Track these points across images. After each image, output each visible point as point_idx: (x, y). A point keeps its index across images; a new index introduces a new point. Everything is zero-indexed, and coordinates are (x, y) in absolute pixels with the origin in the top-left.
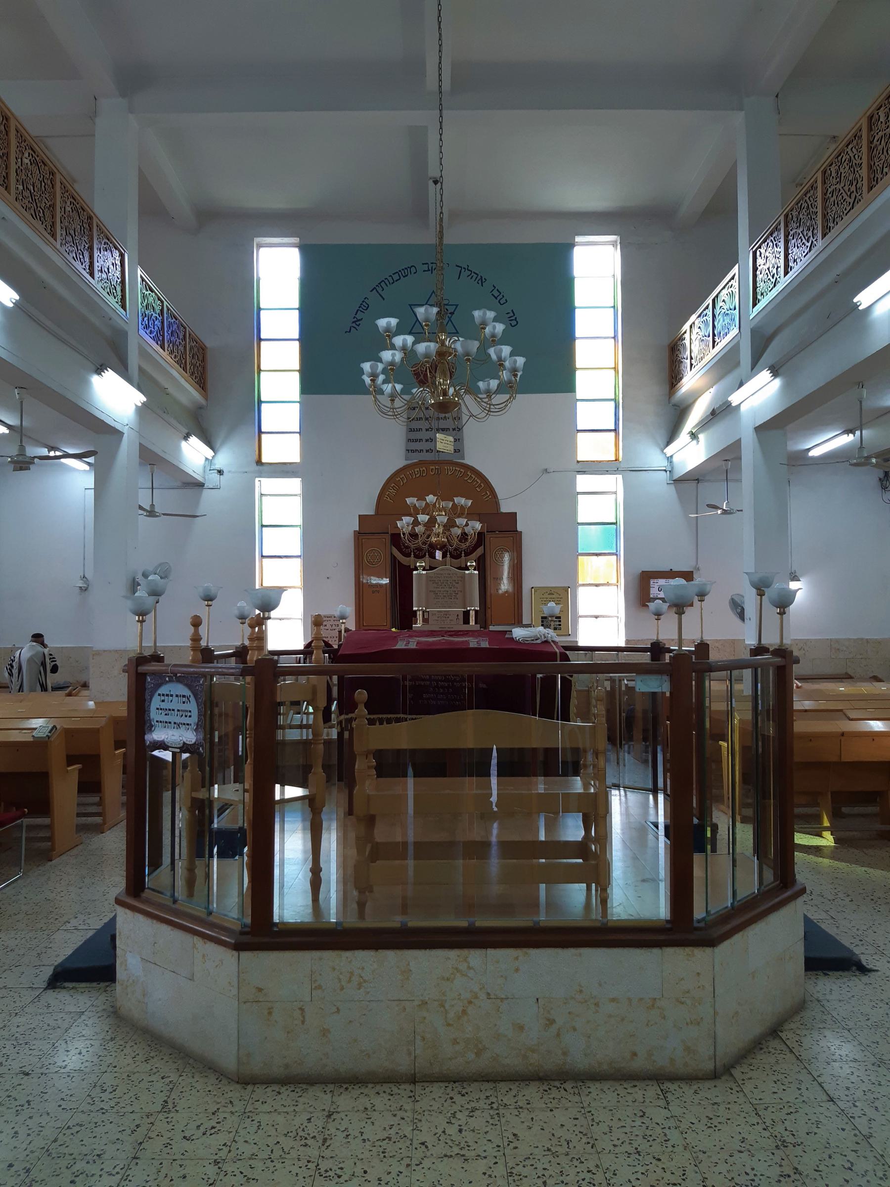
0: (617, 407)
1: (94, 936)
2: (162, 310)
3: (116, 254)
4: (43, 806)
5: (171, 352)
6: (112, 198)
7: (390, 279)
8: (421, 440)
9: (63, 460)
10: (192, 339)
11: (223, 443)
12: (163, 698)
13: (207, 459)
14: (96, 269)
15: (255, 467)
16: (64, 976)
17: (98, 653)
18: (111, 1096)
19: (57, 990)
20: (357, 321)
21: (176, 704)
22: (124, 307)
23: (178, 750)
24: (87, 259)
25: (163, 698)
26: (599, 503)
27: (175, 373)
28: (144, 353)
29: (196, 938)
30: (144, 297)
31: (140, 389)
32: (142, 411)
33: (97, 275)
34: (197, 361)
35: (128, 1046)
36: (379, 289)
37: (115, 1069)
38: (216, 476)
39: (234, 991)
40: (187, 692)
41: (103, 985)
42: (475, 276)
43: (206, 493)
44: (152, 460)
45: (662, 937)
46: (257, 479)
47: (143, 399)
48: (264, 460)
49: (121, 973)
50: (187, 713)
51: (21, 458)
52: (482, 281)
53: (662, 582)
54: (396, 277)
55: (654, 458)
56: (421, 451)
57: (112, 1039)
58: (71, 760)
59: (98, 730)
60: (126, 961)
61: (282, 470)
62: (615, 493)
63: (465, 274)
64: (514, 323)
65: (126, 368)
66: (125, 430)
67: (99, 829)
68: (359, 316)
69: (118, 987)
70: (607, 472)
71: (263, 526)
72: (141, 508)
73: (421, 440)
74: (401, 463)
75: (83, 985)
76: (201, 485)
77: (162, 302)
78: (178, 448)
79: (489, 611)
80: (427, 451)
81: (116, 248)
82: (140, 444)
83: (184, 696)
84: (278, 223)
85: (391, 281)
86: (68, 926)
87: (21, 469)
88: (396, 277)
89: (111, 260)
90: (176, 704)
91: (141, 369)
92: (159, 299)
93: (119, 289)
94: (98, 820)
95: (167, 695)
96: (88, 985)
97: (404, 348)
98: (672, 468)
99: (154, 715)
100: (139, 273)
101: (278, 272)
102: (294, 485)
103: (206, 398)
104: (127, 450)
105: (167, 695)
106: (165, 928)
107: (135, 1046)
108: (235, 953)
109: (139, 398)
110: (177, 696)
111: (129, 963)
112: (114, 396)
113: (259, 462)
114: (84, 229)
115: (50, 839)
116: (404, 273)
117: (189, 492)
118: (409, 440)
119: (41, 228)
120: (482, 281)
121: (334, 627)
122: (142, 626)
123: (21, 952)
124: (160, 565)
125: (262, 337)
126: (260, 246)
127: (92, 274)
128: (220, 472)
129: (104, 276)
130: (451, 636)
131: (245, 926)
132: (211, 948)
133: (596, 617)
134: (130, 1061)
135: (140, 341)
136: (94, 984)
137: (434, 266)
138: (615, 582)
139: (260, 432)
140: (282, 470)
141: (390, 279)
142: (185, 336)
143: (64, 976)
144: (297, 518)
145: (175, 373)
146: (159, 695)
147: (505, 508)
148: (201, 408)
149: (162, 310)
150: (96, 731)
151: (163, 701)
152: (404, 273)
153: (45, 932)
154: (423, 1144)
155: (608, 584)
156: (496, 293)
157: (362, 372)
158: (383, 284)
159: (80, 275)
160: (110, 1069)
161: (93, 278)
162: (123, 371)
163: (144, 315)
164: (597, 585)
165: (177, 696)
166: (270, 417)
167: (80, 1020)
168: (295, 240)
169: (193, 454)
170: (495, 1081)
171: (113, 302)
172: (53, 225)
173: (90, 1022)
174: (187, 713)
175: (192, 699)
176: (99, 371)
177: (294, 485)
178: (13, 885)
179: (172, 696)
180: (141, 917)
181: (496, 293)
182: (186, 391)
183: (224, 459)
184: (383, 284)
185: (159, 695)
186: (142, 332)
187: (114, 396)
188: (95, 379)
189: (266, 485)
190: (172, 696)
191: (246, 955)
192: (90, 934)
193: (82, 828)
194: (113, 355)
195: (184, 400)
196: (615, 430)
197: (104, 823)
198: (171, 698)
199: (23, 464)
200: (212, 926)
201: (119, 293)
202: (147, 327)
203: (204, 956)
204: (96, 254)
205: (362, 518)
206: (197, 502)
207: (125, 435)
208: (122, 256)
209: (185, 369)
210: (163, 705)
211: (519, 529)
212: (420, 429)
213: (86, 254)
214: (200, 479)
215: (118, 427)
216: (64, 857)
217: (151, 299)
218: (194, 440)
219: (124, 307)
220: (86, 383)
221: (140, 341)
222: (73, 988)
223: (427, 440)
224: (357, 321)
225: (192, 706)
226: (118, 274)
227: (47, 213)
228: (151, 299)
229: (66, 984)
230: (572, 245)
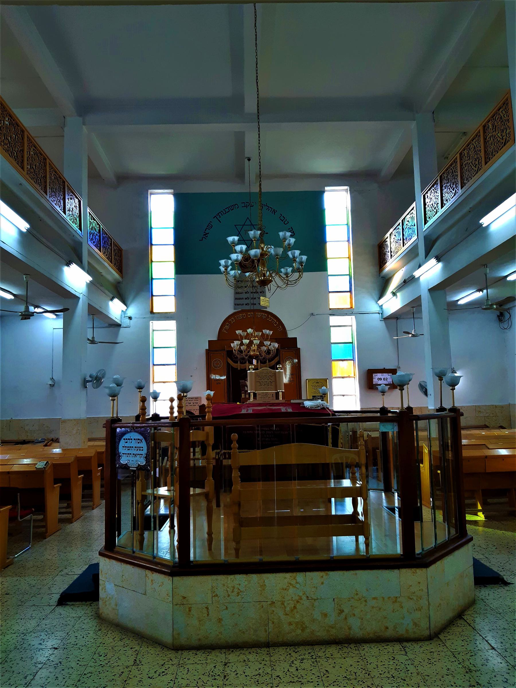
0: (350, 279)
1: (77, 579)
2: (100, 230)
3: (77, 200)
4: (41, 508)
5: (104, 253)
6: (75, 172)
7: (224, 211)
8: (242, 299)
9: (44, 314)
10: (115, 245)
11: (131, 302)
12: (126, 441)
13: (122, 311)
14: (67, 209)
15: (149, 315)
16: (66, 599)
17: (64, 421)
18: (105, 658)
19: (64, 606)
21: (134, 444)
22: (80, 229)
23: (135, 469)
24: (62, 205)
25: (126, 441)
26: (342, 331)
27: (106, 264)
28: (91, 254)
29: (147, 571)
30: (90, 223)
31: (89, 273)
32: (90, 286)
33: (67, 212)
34: (118, 257)
35: (109, 633)
36: (218, 217)
37: (104, 645)
38: (128, 320)
39: (170, 599)
40: (140, 437)
41: (88, 603)
42: (271, 209)
43: (122, 330)
44: (95, 313)
45: (399, 563)
46: (151, 322)
47: (91, 279)
48: (155, 311)
49: (102, 594)
50: (140, 448)
51: (26, 313)
52: (274, 212)
53: (379, 375)
55: (372, 306)
56: (243, 304)
57: (100, 630)
58: (56, 481)
59: (69, 464)
60: (105, 587)
61: (165, 316)
62: (351, 326)
63: (265, 208)
65: (81, 262)
66: (81, 296)
67: (70, 521)
68: (207, 232)
69: (101, 602)
70: (346, 314)
71: (154, 348)
72: (88, 339)
73: (242, 299)
74: (230, 311)
75: (78, 603)
76: (119, 326)
77: (100, 226)
78: (107, 305)
80: (246, 304)
81: (77, 198)
82: (89, 305)
83: (139, 439)
84: (162, 182)
86: (63, 573)
87: (25, 319)
89: (74, 204)
90: (134, 444)
91: (89, 263)
92: (98, 224)
93: (78, 219)
94: (69, 516)
95: (129, 439)
96: (80, 603)
97: (241, 252)
98: (383, 312)
99: (121, 450)
100: (88, 210)
101: (162, 208)
102: (172, 324)
103: (122, 277)
104: (81, 308)
105: (129, 439)
106: (129, 567)
107: (113, 633)
108: (171, 578)
109: (89, 278)
110: (135, 439)
111: (107, 588)
112: (75, 278)
113: (152, 312)
114: (62, 188)
115: (45, 526)
116: (232, 208)
117: (116, 329)
118: (236, 299)
119: (39, 188)
120: (274, 212)
121: (195, 404)
122: (113, 402)
123: (39, 587)
124: (99, 371)
125: (153, 243)
126: (151, 194)
127: (65, 213)
128: (130, 318)
129: (71, 213)
130: (270, 406)
131: (175, 563)
132: (156, 576)
133: (343, 396)
134: (112, 640)
135: (89, 247)
136: (84, 603)
138: (353, 375)
139: (152, 296)
140: (165, 316)
141: (224, 211)
142: (111, 244)
143: (66, 599)
144: (173, 342)
145: (106, 264)
146: (124, 439)
147: (290, 335)
148: (119, 283)
149: (100, 230)
150: (69, 465)
151: (127, 442)
152: (232, 208)
153: (51, 576)
154: (278, 676)
155: (349, 377)
156: (283, 219)
157: (220, 265)
158: (220, 214)
159: (58, 213)
160: (101, 645)
161: (65, 214)
162: (80, 264)
163: (90, 233)
164: (343, 378)
165: (135, 439)
166: (157, 287)
167: (80, 621)
168: (171, 191)
169: (115, 308)
170: (312, 645)
171: (75, 227)
172: (45, 187)
173: (85, 622)
174: (140, 448)
175: (143, 440)
176: (68, 264)
177: (172, 324)
178: (28, 552)
179: (131, 439)
180: (114, 562)
181: (283, 219)
182: (111, 273)
183: (132, 311)
184: (220, 214)
185: (124, 439)
186: (89, 242)
187: (75, 278)
188: (66, 269)
189: (155, 325)
190: (131, 439)
191: (176, 579)
192: (76, 577)
193: (61, 521)
194: (74, 255)
195: (109, 278)
196: (350, 291)
197: (73, 517)
198: (131, 441)
199: (27, 316)
200: (157, 564)
201: (78, 222)
202: (92, 239)
203: (152, 581)
204: (67, 201)
206: (116, 335)
207: (81, 300)
208: (80, 202)
209: (111, 262)
210: (126, 445)
211: (298, 347)
213: (62, 202)
214: (119, 322)
215: (77, 295)
216: (52, 537)
217: (94, 224)
218: (116, 301)
219: (80, 229)
220: (61, 271)
221: (89, 247)
222: (72, 605)
225: (144, 444)
226: (78, 212)
227: (42, 181)
228: (94, 224)
229: (68, 603)
230: (324, 192)
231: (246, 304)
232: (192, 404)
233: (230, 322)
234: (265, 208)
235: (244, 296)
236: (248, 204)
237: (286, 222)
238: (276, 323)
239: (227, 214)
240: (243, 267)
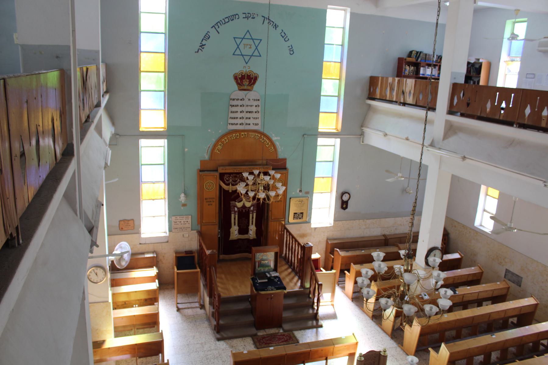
0: (339, 101)
8: (237, 118)
20: (202, 46)
36: (217, 27)
42: (272, 23)
52: (276, 27)
54: (227, 20)
56: (237, 124)
64: (292, 52)
68: (204, 43)
73: (237, 118)
79: (270, 213)
80: (240, 124)
85: (224, 22)
88: (227, 20)
120: (276, 27)
137: (249, 15)
147: (281, 156)
156: (283, 35)
158: (219, 24)
177: (163, 142)
181: (283, 35)
205: (202, 162)
212: (237, 112)
223: (240, 118)
224: (202, 46)
230: (325, 12)
231: (240, 124)
232: (182, 222)
233: (223, 142)
234: (266, 21)
235: (239, 115)
236: (249, 15)
237: (286, 40)
238: (268, 144)
239: (226, 24)
240: (240, 84)
